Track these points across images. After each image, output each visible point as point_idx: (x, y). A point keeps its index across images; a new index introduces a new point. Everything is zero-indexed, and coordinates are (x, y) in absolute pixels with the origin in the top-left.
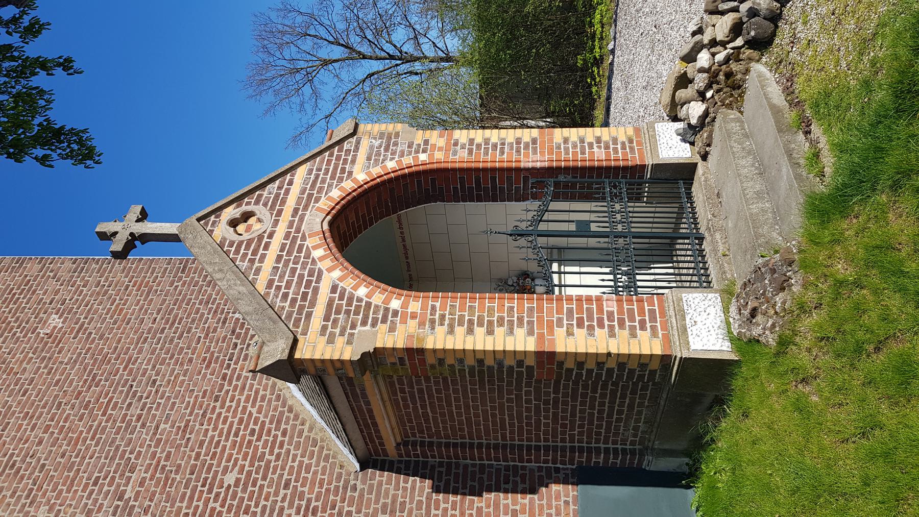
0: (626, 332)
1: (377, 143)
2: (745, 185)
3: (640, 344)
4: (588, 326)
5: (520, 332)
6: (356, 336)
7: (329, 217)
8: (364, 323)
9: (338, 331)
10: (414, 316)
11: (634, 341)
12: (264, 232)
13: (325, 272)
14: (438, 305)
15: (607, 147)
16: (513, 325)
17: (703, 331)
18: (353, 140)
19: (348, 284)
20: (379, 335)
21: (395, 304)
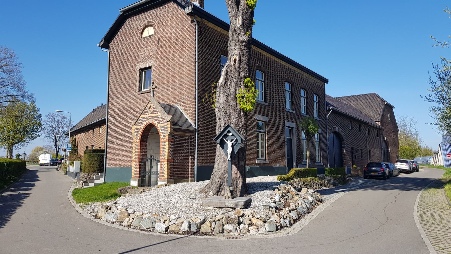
19: (141, 130)
21: (138, 138)
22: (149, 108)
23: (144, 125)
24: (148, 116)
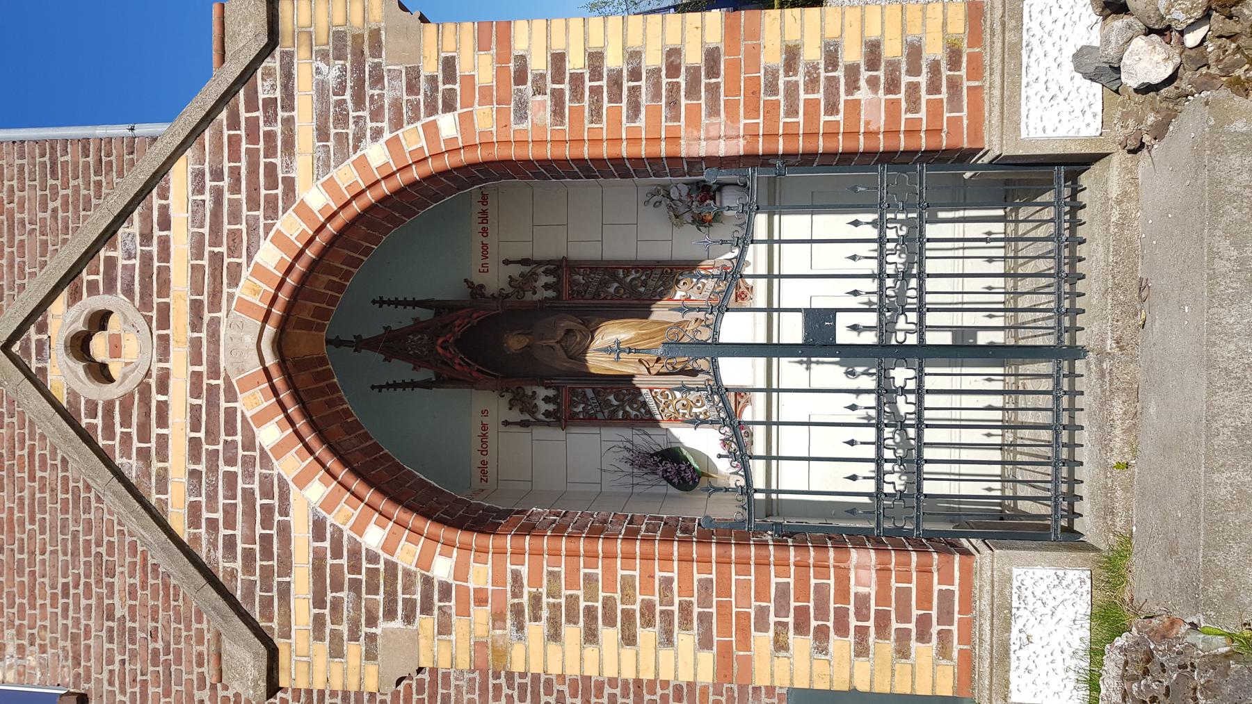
0: (889, 646)
1: (331, 73)
2: (1218, 400)
3: (913, 674)
4: (817, 629)
5: (686, 640)
6: (379, 641)
7: (270, 330)
8: (390, 614)
9: (344, 628)
10: (481, 601)
11: (903, 667)
12: (148, 374)
13: (292, 486)
14: (524, 570)
15: (893, 86)
16: (671, 623)
17: (1041, 662)
18: (273, 62)
19: (344, 516)
20: (422, 642)
22: (101, 373)
23: (290, 465)
24: (179, 398)
